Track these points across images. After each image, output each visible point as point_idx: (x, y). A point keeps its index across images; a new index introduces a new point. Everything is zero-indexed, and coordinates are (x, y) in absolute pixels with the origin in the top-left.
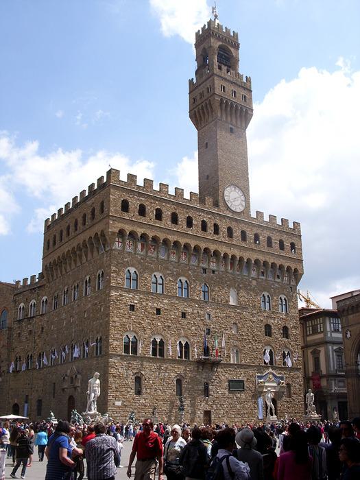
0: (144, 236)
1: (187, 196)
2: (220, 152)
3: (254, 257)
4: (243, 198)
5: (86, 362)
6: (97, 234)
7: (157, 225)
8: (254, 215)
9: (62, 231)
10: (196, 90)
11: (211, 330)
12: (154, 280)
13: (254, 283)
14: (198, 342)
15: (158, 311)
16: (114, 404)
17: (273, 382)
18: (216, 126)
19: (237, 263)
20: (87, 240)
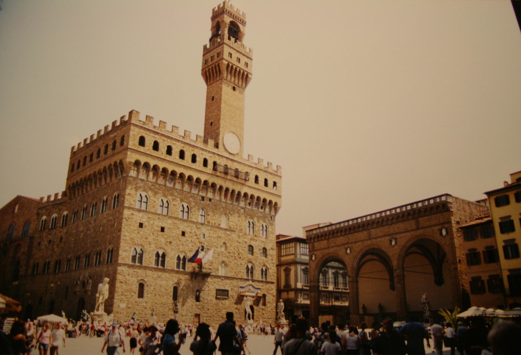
2: (223, 105)
4: (238, 142)
5: (98, 269)
6: (116, 162)
7: (167, 159)
9: (85, 158)
10: (209, 54)
11: (205, 247)
16: (119, 306)
17: (252, 292)
18: (221, 84)
19: (229, 194)
20: (107, 166)
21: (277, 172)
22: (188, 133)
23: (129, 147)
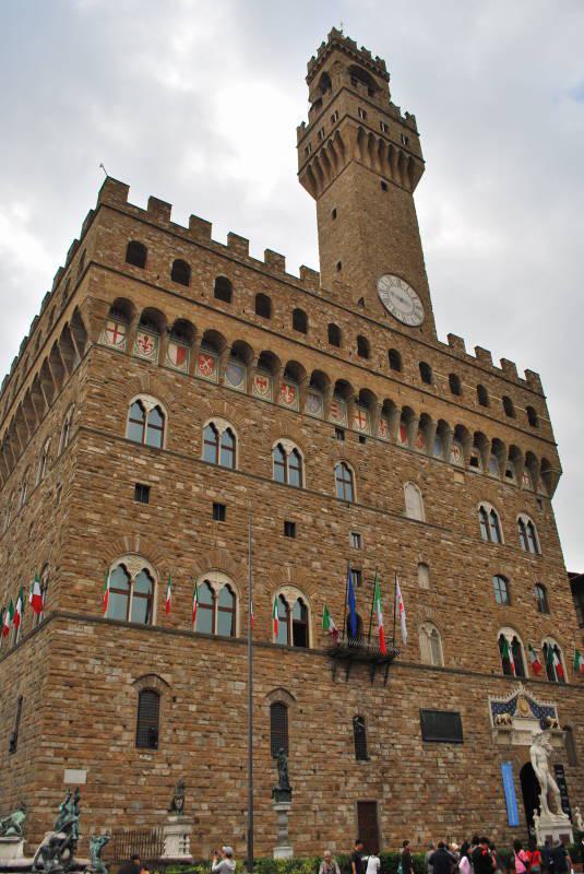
0: (183, 330)
1: (292, 269)
3: (455, 418)
4: (418, 302)
8: (443, 338)
12: (209, 435)
13: (459, 478)
14: (333, 601)
15: (219, 510)
16: (60, 778)
19: (415, 426)
21: (528, 383)
22: (278, 258)
23: (95, 261)
